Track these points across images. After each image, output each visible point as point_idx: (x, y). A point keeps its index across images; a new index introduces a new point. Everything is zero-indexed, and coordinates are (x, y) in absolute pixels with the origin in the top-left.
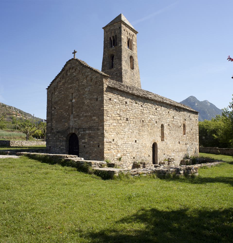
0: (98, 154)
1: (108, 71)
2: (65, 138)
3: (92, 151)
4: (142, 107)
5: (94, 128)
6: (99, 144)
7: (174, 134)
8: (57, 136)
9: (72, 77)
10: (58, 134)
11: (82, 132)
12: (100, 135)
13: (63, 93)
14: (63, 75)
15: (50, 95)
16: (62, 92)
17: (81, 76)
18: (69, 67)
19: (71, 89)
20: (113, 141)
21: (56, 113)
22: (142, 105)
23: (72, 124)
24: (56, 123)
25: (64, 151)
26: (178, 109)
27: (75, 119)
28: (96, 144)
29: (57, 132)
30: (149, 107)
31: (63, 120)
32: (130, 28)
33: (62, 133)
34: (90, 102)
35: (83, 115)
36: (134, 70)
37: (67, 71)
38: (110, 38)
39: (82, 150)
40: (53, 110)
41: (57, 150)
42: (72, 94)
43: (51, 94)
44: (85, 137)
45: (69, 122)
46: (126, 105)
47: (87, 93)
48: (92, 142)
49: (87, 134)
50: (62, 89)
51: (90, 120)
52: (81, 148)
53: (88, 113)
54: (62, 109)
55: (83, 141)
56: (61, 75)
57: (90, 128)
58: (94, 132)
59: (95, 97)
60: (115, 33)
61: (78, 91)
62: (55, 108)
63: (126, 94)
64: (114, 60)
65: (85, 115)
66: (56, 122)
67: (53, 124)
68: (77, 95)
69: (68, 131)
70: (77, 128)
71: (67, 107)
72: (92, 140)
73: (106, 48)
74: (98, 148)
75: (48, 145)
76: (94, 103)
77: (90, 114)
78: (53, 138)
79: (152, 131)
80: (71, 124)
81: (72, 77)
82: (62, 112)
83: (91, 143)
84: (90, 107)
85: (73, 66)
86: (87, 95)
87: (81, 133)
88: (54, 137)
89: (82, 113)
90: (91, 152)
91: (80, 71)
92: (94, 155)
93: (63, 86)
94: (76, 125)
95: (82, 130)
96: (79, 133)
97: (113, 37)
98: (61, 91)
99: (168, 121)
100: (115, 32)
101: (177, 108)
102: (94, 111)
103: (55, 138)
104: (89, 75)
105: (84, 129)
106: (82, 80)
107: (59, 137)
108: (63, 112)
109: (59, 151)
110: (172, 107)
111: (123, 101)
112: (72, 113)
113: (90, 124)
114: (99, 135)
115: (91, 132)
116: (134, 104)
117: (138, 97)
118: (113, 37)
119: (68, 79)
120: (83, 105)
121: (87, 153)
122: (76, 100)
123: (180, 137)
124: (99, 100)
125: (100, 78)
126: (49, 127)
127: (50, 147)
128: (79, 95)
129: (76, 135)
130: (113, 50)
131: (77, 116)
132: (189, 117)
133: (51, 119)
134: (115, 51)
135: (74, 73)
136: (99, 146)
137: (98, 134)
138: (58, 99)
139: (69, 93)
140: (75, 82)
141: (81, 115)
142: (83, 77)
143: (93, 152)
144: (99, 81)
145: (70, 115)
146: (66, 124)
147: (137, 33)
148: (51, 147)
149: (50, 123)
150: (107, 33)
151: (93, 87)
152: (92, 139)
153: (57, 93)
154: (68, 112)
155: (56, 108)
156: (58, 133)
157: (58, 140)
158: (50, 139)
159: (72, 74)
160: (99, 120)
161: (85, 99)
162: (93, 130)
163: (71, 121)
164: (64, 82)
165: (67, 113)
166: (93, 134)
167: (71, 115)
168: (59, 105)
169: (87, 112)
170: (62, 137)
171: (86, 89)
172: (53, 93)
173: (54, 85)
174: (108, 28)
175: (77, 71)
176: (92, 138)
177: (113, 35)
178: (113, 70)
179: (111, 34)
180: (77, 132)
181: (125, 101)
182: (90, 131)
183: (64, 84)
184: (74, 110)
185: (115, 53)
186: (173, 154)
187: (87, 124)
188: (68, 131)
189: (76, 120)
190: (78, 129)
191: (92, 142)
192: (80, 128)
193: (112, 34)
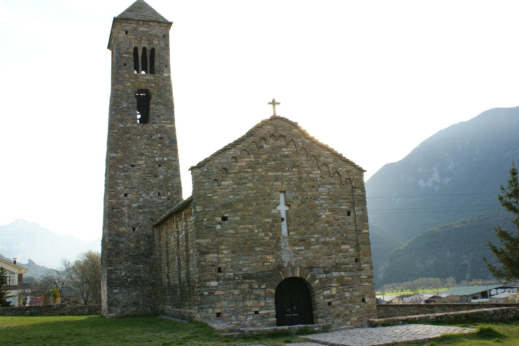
1: (134, 125)
2: (274, 291)
3: (350, 312)
5: (346, 266)
6: (363, 296)
8: (245, 286)
9: (278, 155)
10: (247, 281)
15: (205, 184)
17: (305, 161)
18: (269, 132)
21: (231, 231)
23: (289, 258)
25: (270, 319)
27: (297, 249)
28: (359, 296)
31: (259, 249)
33: (261, 277)
35: (317, 241)
38: (136, 50)
39: (326, 312)
40: (220, 223)
41: (249, 319)
44: (331, 285)
45: (279, 253)
47: (323, 197)
48: (347, 294)
49: (335, 279)
51: (336, 251)
52: (322, 309)
53: (331, 238)
55: (326, 293)
56: (243, 144)
57: (337, 267)
59: (344, 207)
60: (150, 43)
61: (300, 189)
64: (152, 106)
65: (323, 240)
66: (233, 252)
67: (221, 256)
68: (297, 198)
69: (281, 273)
72: (347, 289)
73: (125, 69)
75: (210, 311)
76: (343, 219)
77: (334, 239)
78: (230, 293)
80: (286, 258)
82: (251, 231)
84: (333, 226)
86: (323, 201)
88: (235, 288)
89: (316, 236)
90: (347, 312)
92: (355, 319)
93: (249, 170)
94: (300, 260)
96: (314, 278)
97: (144, 49)
98: (243, 181)
100: (153, 40)
102: (344, 235)
103: (236, 292)
104: (329, 163)
107: (251, 287)
108: (256, 231)
109: (255, 321)
113: (336, 258)
118: (144, 49)
121: (338, 316)
125: (356, 175)
126: (213, 266)
128: (302, 197)
129: (307, 282)
130: (148, 80)
131: (299, 241)
134: (153, 85)
135: (284, 149)
136: (363, 300)
137: (360, 278)
138: (237, 197)
139: (271, 190)
140: (287, 169)
143: (353, 312)
144: (354, 179)
145: (279, 239)
146: (267, 257)
149: (213, 253)
150: (126, 33)
151: (338, 186)
152: (349, 288)
153: (231, 182)
154: (271, 232)
155: (229, 218)
158: (216, 294)
159: (274, 149)
162: (350, 271)
163: (283, 252)
166: (350, 278)
168: (239, 213)
169: (328, 235)
171: (320, 189)
173: (222, 161)
174: (131, 25)
176: (347, 287)
177: (145, 44)
178: (151, 127)
179: (141, 41)
180: (309, 276)
182: (343, 273)
183: (252, 166)
185: (156, 90)
187: (329, 259)
189: (299, 250)
190: (311, 268)
191: (347, 294)
193: (143, 42)
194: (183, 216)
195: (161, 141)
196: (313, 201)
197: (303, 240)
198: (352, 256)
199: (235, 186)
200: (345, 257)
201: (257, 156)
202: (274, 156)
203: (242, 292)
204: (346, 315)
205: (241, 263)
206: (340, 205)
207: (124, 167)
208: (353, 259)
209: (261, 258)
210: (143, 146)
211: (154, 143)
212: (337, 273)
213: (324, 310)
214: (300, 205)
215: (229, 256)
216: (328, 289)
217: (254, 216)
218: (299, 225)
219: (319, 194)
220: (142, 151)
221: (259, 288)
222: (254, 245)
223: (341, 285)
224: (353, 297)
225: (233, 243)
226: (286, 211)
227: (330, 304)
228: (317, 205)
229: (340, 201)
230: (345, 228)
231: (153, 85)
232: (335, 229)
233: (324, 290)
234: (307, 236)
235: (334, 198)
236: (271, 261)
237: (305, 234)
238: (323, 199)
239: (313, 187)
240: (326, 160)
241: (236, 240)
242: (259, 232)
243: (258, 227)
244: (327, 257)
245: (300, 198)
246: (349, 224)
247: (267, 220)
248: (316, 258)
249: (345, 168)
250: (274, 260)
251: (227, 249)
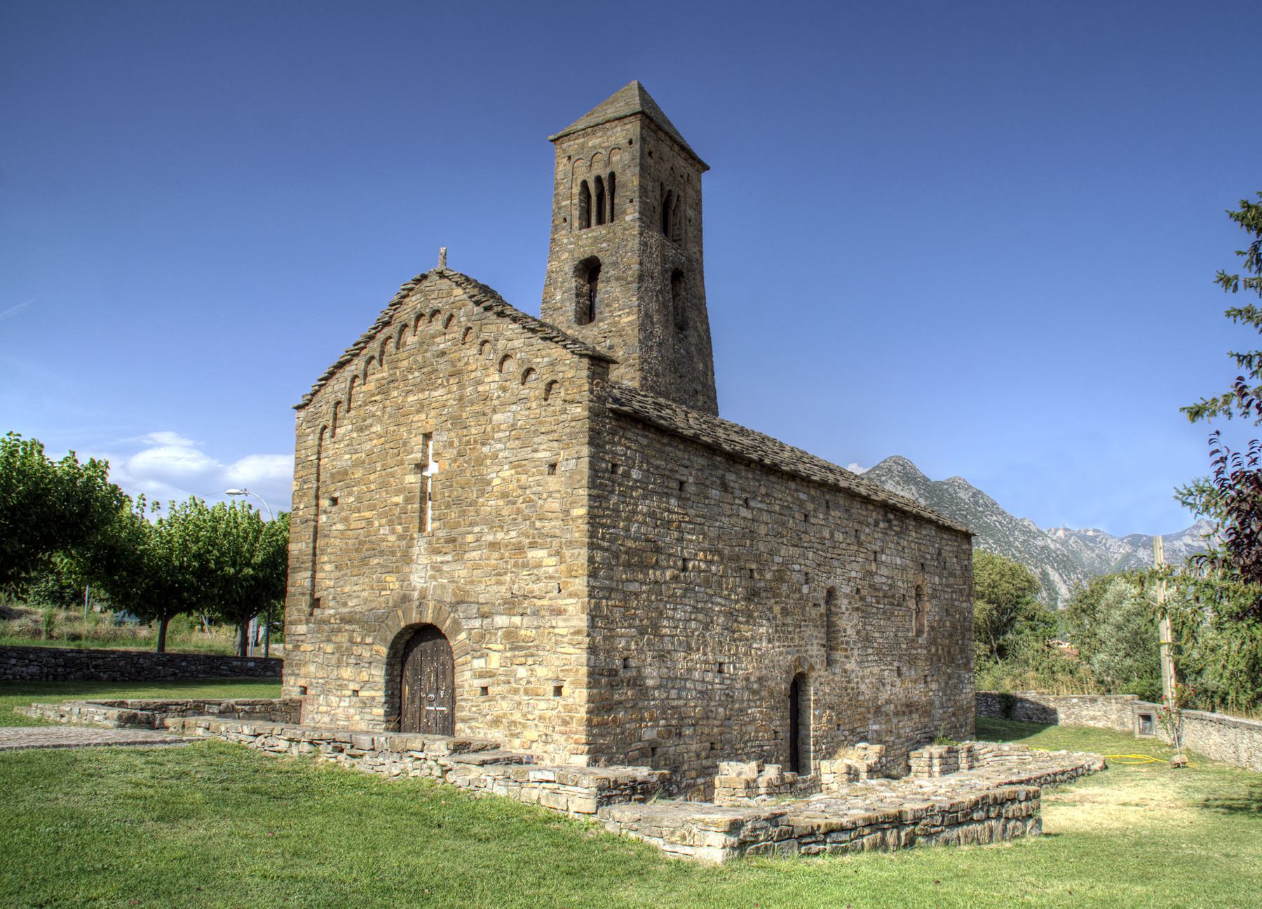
0: (557, 728)
4: (748, 507)
6: (558, 679)
7: (877, 635)
8: (343, 638)
10: (347, 627)
12: (566, 640)
13: (377, 428)
14: (384, 343)
16: (371, 426)
19: (418, 412)
20: (625, 667)
21: (340, 526)
22: (746, 501)
24: (338, 574)
26: (896, 519)
29: (342, 619)
30: (777, 508)
31: (375, 561)
32: (676, 148)
33: (368, 622)
34: (518, 481)
36: (691, 332)
37: (405, 326)
39: (474, 709)
40: (325, 512)
41: (342, 704)
42: (427, 436)
43: (319, 431)
46: (679, 498)
47: (501, 435)
48: (522, 672)
49: (500, 633)
50: (374, 409)
51: (516, 565)
54: (372, 508)
55: (479, 664)
57: (512, 604)
60: (609, 162)
61: (457, 422)
62: (335, 501)
63: (681, 446)
64: (600, 286)
65: (490, 538)
68: (451, 444)
69: (400, 613)
70: (448, 600)
71: (399, 499)
72: (523, 660)
73: (563, 228)
74: (557, 698)
75: (292, 680)
77: (513, 534)
79: (789, 620)
80: (418, 579)
81: (428, 354)
82: (369, 522)
83: (519, 676)
84: (514, 503)
85: (436, 304)
87: (466, 625)
88: (329, 641)
89: (477, 529)
90: (517, 716)
91: (468, 329)
93: (377, 398)
94: (443, 587)
95: (475, 611)
96: (457, 628)
97: (598, 180)
98: (368, 422)
99: (853, 574)
101: (891, 516)
102: (538, 524)
103: (329, 648)
105: (486, 609)
106: (479, 374)
107: (351, 641)
108: (376, 523)
109: (352, 711)
110: (871, 507)
111: (668, 477)
112: (422, 529)
114: (563, 636)
116: (715, 493)
117: (735, 462)
119: (405, 363)
120: (482, 493)
122: (447, 467)
123: (904, 646)
124: (560, 469)
125: (571, 368)
126: (303, 594)
127: (304, 690)
130: (595, 237)
131: (447, 542)
132: (939, 554)
133: (314, 554)
134: (604, 245)
135: (438, 340)
136: (558, 691)
138: (354, 457)
139: (409, 432)
141: (470, 538)
142: (483, 357)
143: (530, 717)
145: (412, 539)
146: (388, 579)
147: (706, 168)
148: (309, 691)
149: (306, 569)
150: (569, 158)
151: (534, 405)
152: (526, 656)
153: (350, 427)
154: (400, 524)
156: (349, 622)
160: (563, 567)
161: (488, 462)
164: (384, 378)
165: (399, 529)
167: (415, 536)
169: (502, 527)
170: (369, 640)
171: (498, 417)
172: (325, 427)
173: (336, 388)
175: (456, 332)
180: (448, 622)
181: (678, 476)
182: (517, 620)
183: (383, 390)
184: (430, 513)
186: (876, 727)
187: (499, 583)
188: (400, 613)
190: (455, 605)
192: (463, 602)
193: (595, 166)
196: (479, 446)
197: (454, 540)
198: (551, 578)
199: (355, 435)
200: (534, 578)
201: (394, 365)
202: (420, 358)
203: (338, 648)
204: (514, 723)
205: (346, 590)
206: (536, 451)
208: (553, 584)
209: (379, 581)
213: (470, 704)
214: (455, 461)
216: (482, 656)
218: (448, 506)
219: (493, 429)
221: (363, 643)
223: (511, 649)
224: (532, 679)
227: (485, 690)
228: (486, 457)
229: (535, 440)
230: (542, 506)
231: (604, 245)
232: (519, 511)
233: (474, 658)
234: (459, 530)
235: (522, 435)
236: (391, 586)
237: (457, 525)
238: (500, 440)
239: (484, 414)
240: (510, 345)
242: (380, 526)
243: (380, 516)
244: (494, 579)
245: (456, 443)
246: (550, 494)
248: (472, 582)
249: (549, 355)
250: (397, 585)
251: (330, 562)
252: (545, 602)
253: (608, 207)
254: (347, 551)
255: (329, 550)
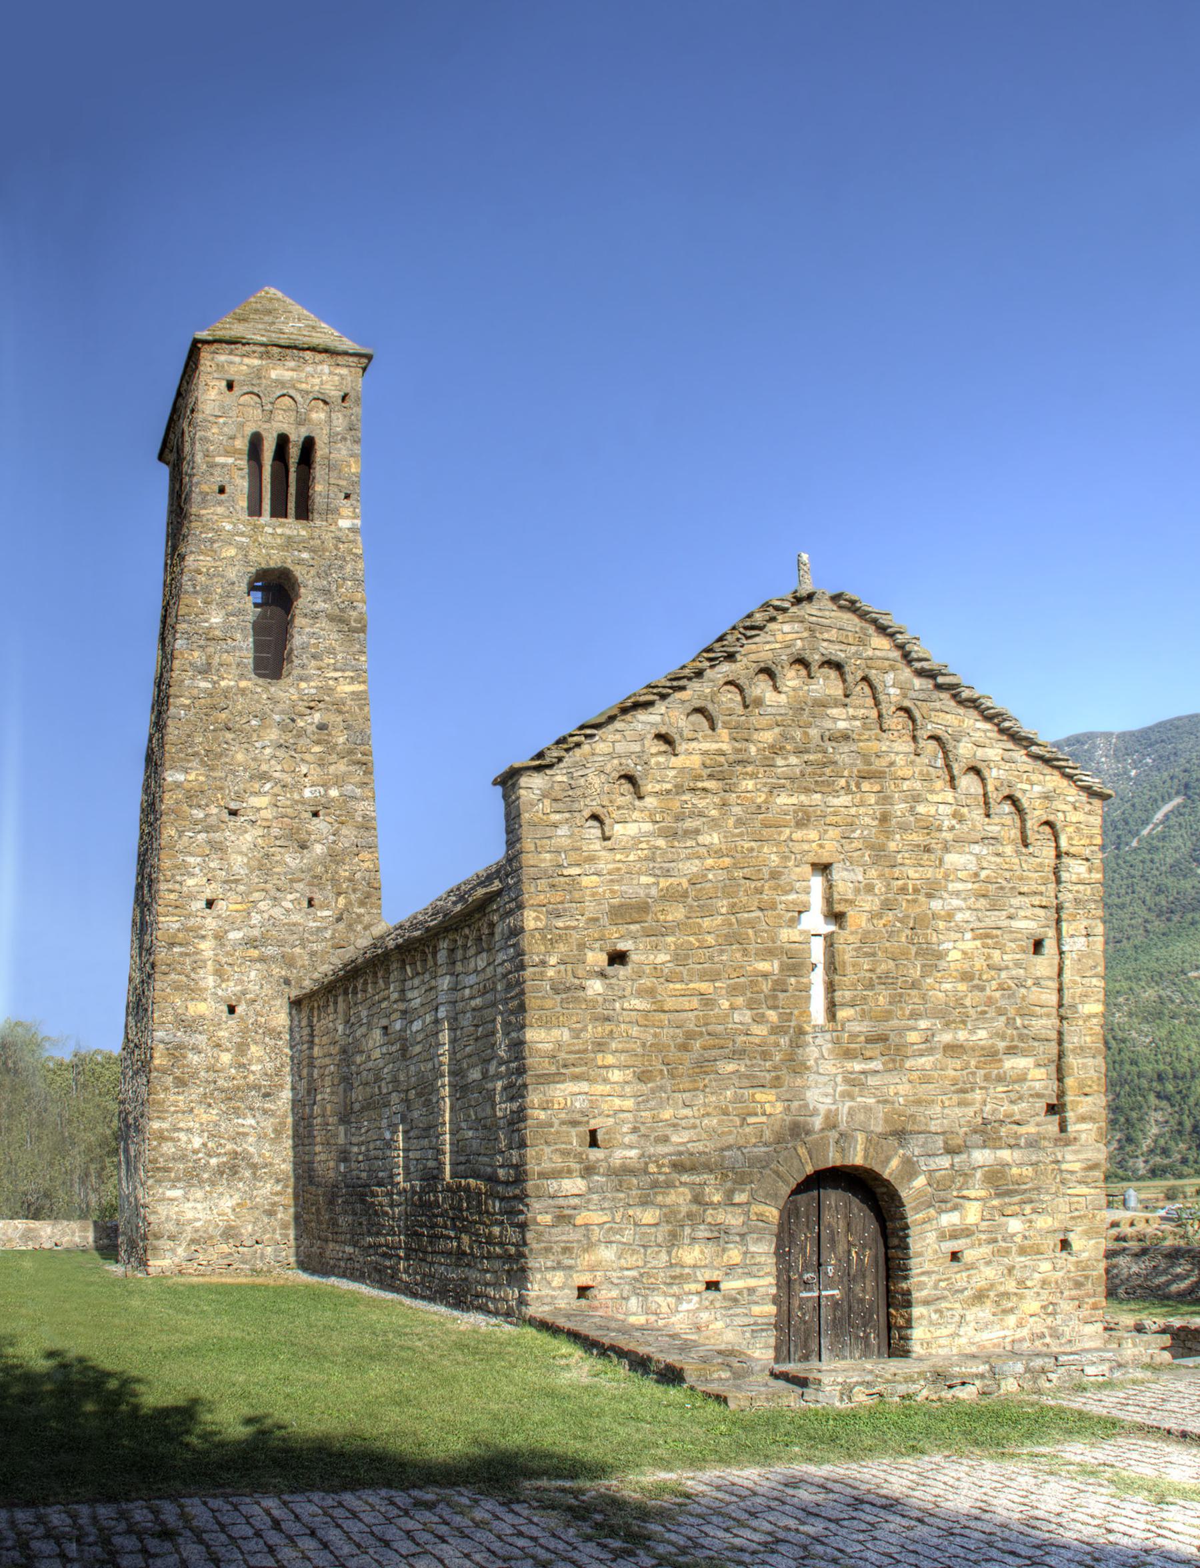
5: (1015, 1127)
11: (937, 1160)
24: (645, 1088)
54: (713, 977)
58: (1034, 1158)
66: (643, 1077)
67: (600, 1088)
82: (707, 1002)
115: (1009, 1160)
154: (775, 1008)
157: (693, 1227)
166: (1028, 1171)
182: (1005, 1155)
194: (442, 956)
195: (323, 735)
207: (207, 815)
209: (738, 1099)
210: (268, 751)
211: (303, 741)
212: (987, 1152)
215: (628, 1089)
217: (722, 952)
220: (264, 767)
222: (715, 1052)
225: (644, 1045)
226: (830, 940)
241: (655, 1035)
242: (733, 1008)
243: (733, 991)
247: (764, 966)
252: (1032, 1129)
253: (292, 490)
254: (658, 1047)
255: (614, 1045)
